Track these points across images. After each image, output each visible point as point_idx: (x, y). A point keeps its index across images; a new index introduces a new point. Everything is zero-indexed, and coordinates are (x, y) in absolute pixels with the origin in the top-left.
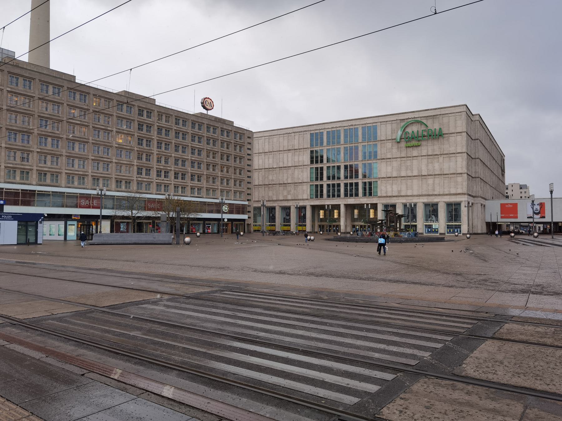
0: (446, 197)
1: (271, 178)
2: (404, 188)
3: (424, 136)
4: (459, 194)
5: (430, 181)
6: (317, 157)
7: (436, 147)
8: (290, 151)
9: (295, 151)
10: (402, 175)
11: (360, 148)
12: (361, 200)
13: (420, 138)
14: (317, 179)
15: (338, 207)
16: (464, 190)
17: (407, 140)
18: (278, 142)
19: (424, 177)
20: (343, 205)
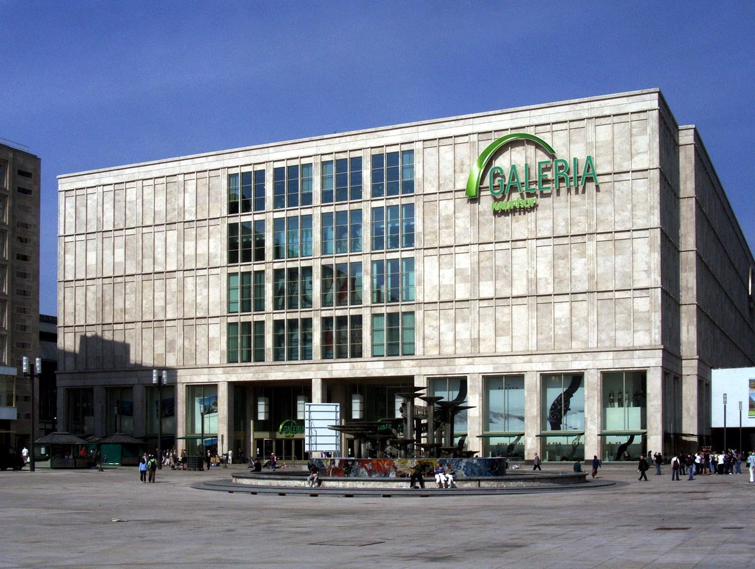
2: (487, 330)
5: (561, 310)
6: (247, 245)
9: (187, 225)
10: (483, 295)
11: (367, 217)
14: (246, 308)
15: (303, 388)
18: (140, 201)
19: (544, 300)
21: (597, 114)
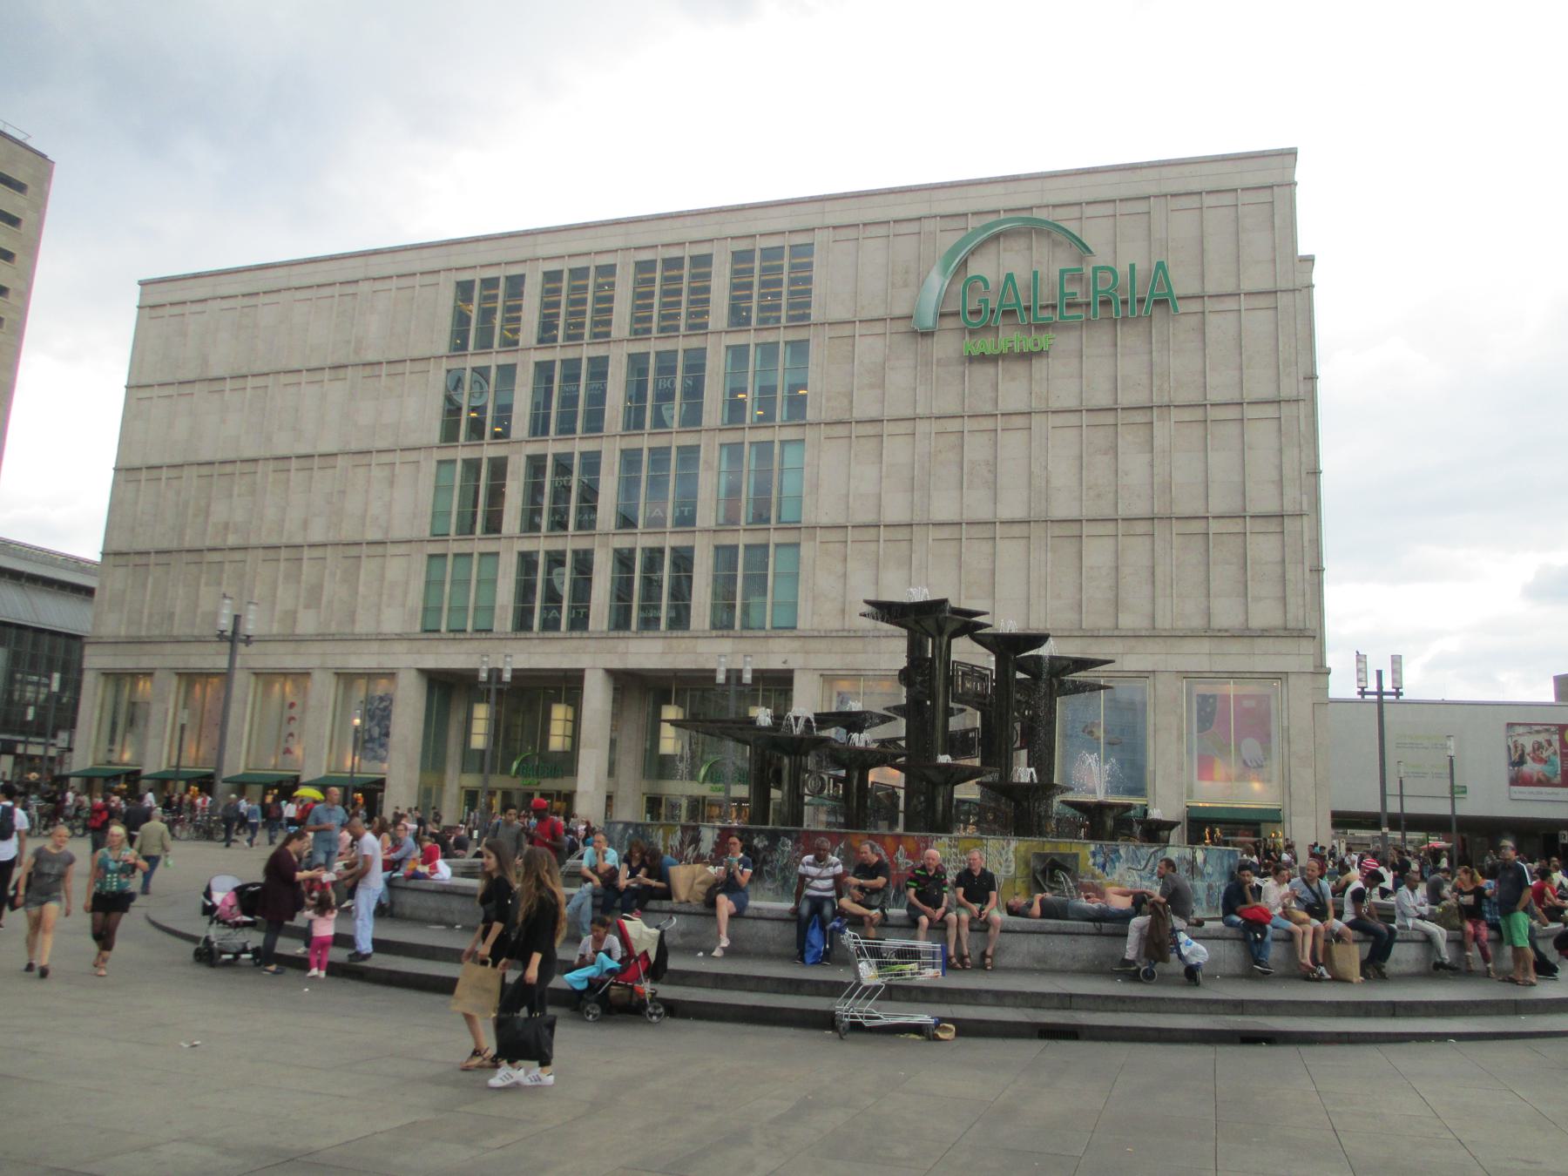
0: (1190, 646)
1: (219, 512)
3: (1069, 306)
4: (1264, 634)
7: (1131, 367)
8: (341, 373)
12: (703, 646)
13: (1047, 314)
14: (466, 528)
15: (568, 685)
17: (974, 320)
20: (600, 674)
21: (1175, 189)
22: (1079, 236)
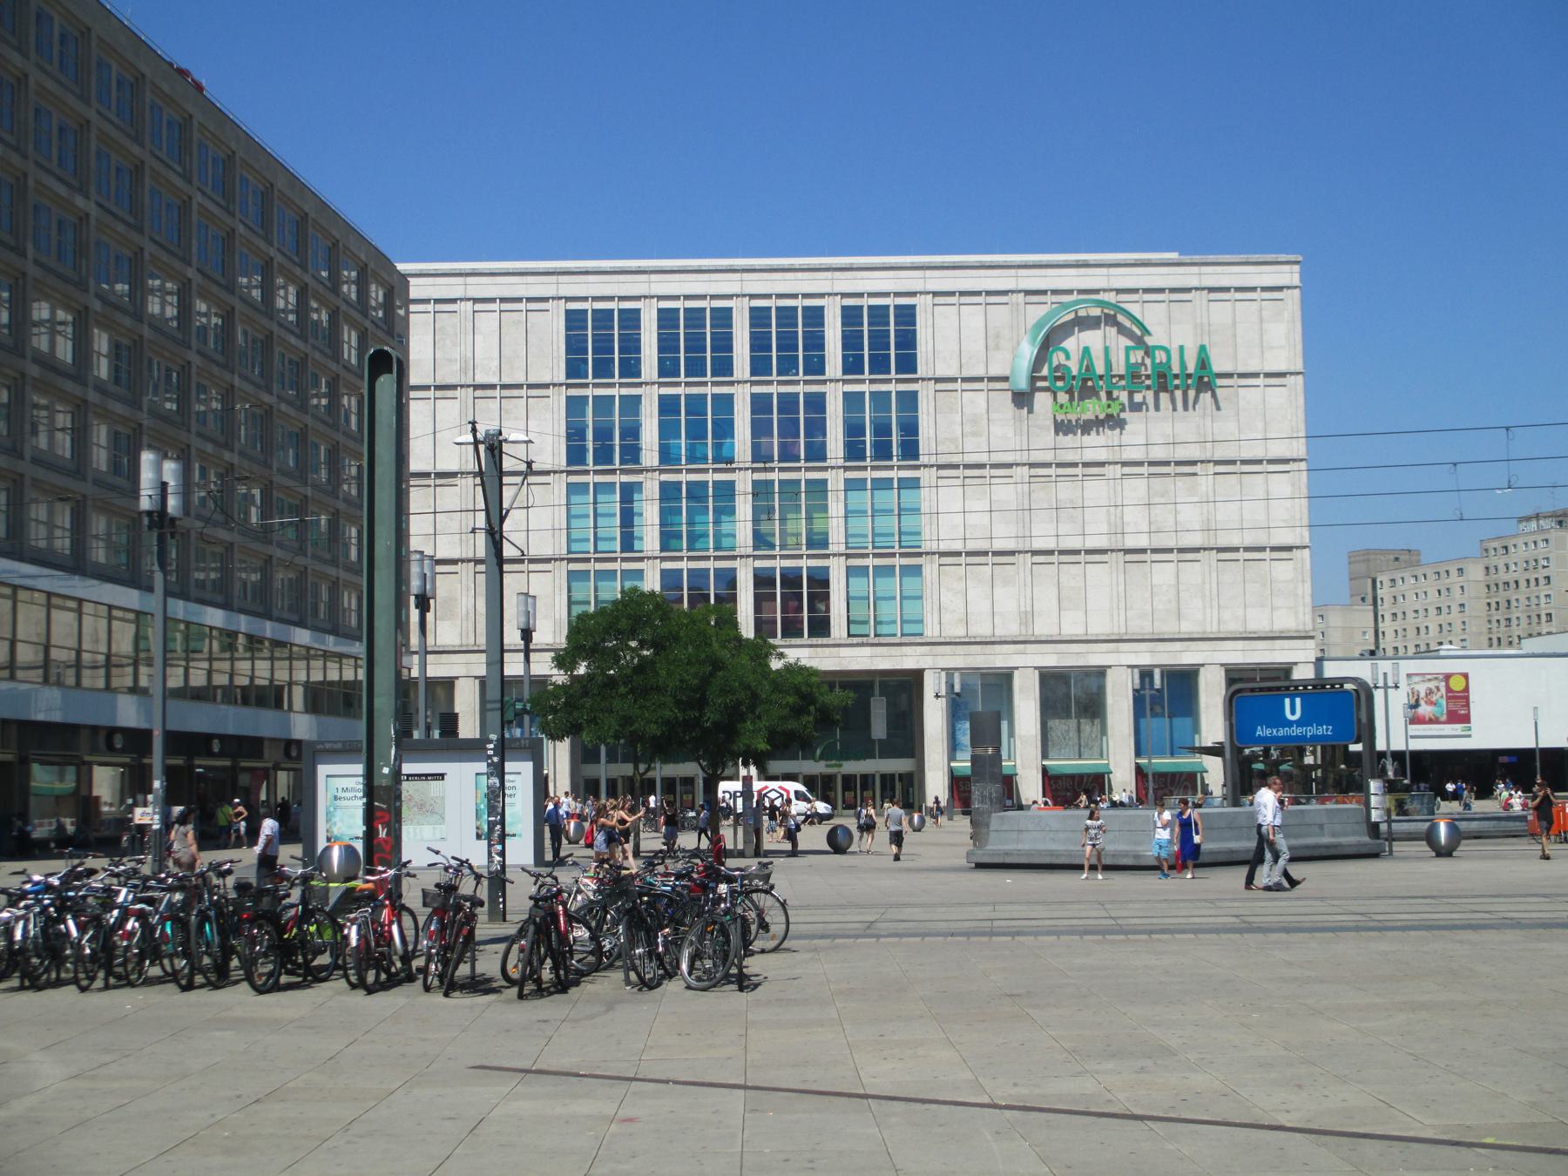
2: (1046, 598)
5: (1163, 573)
16: (1301, 617)
22: (1141, 320)
